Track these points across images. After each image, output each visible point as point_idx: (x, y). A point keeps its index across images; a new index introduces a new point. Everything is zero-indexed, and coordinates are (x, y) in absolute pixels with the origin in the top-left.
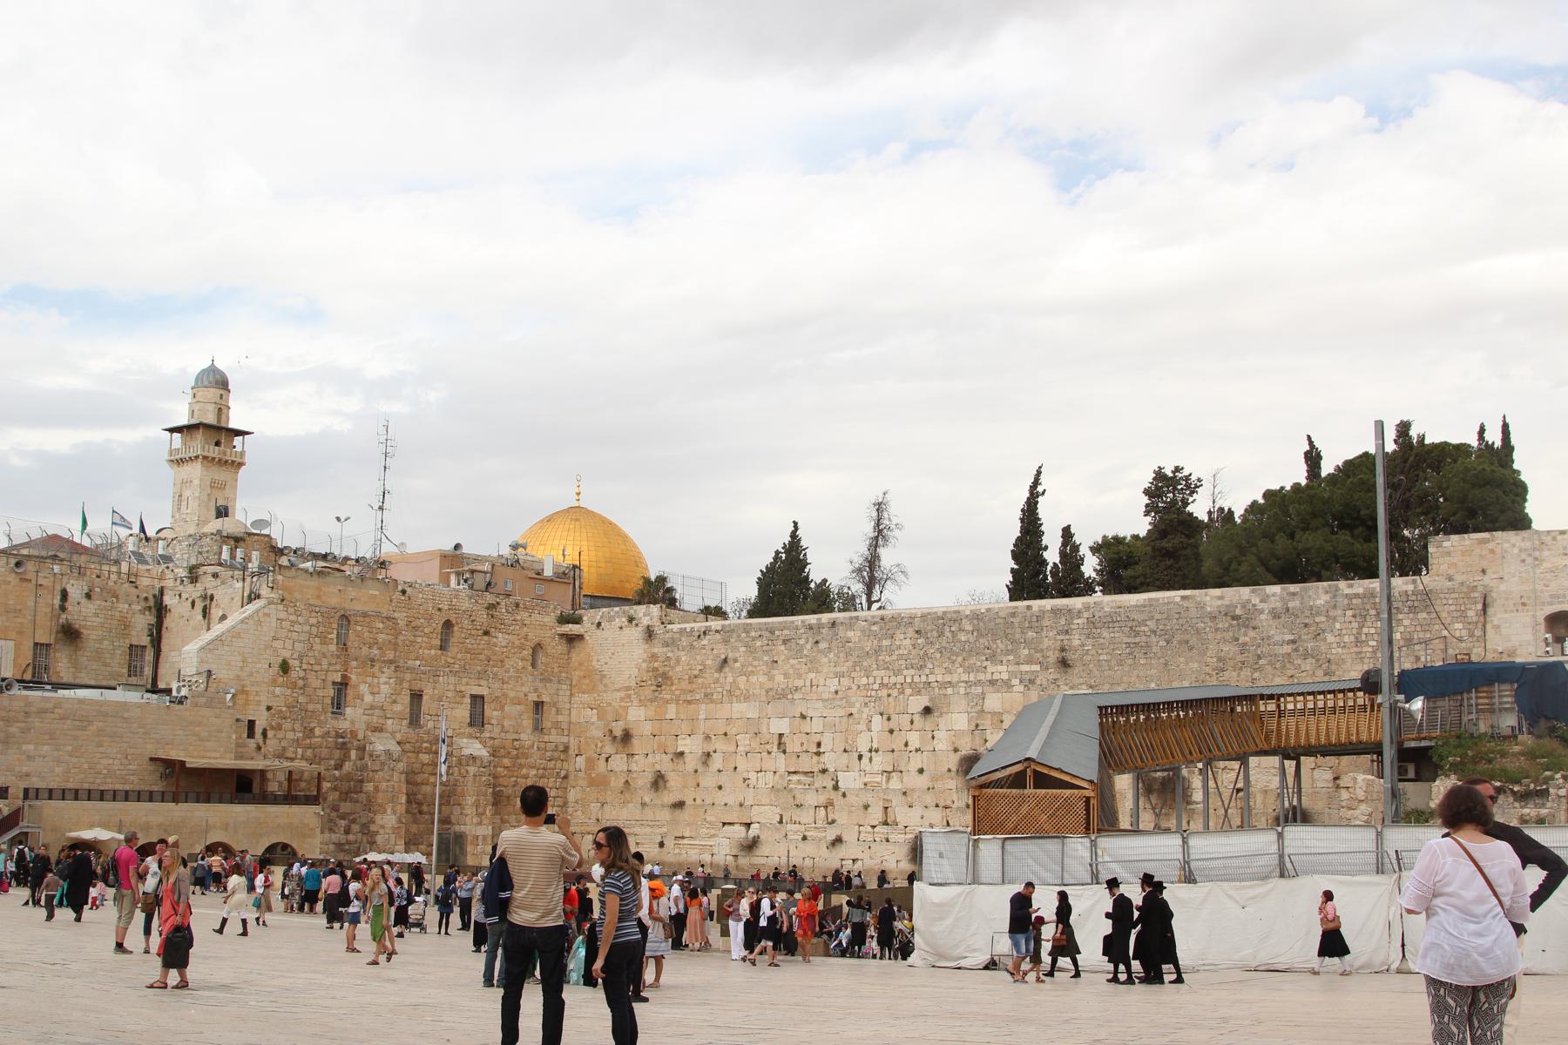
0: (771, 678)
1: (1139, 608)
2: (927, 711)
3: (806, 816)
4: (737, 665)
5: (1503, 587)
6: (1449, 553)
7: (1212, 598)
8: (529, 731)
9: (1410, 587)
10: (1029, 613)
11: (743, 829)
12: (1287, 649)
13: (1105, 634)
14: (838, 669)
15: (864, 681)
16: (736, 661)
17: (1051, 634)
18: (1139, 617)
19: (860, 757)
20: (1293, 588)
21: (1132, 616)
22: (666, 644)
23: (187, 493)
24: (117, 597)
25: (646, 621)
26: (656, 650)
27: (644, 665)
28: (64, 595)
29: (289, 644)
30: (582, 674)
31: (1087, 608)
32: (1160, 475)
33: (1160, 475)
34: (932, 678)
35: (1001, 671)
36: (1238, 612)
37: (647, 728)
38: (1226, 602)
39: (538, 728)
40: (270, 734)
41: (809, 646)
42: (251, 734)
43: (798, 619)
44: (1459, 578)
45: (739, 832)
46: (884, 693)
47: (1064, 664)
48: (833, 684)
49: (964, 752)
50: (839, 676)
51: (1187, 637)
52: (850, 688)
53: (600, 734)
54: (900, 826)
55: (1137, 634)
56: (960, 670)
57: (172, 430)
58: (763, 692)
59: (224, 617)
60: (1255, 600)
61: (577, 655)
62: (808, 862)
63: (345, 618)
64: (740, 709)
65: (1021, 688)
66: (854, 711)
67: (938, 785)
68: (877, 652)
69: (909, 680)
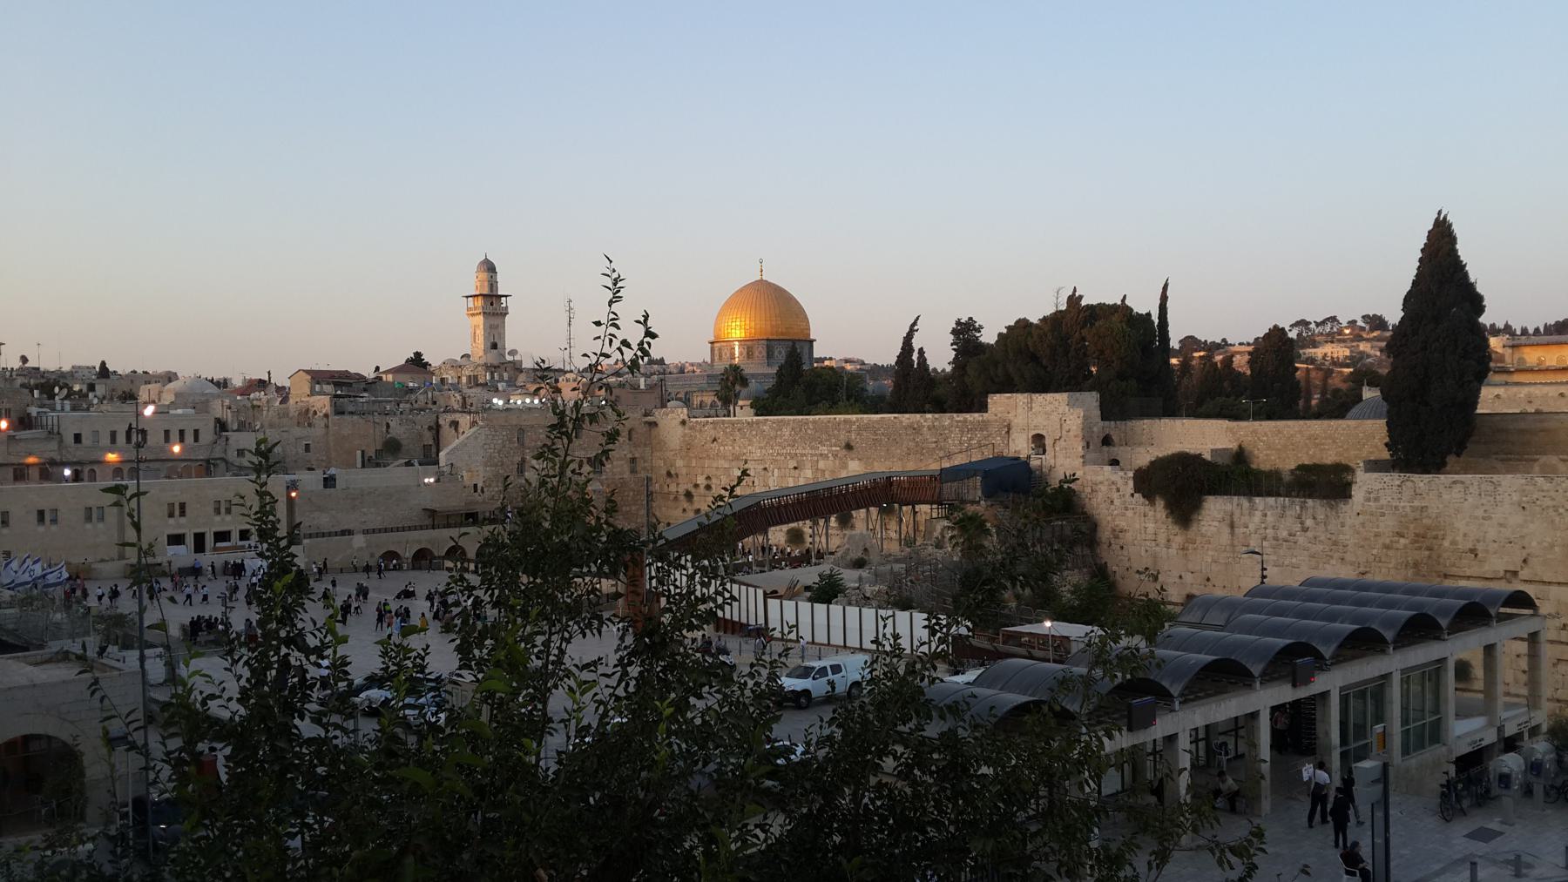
1: (877, 422)
2: (795, 468)
7: (906, 418)
8: (628, 473)
12: (934, 445)
20: (937, 416)
22: (691, 429)
23: (478, 332)
28: (388, 426)
29: (492, 446)
31: (857, 420)
32: (958, 323)
33: (958, 323)
35: (824, 450)
37: (684, 471)
39: (633, 471)
40: (485, 490)
42: (476, 491)
44: (999, 415)
46: (779, 458)
50: (761, 448)
55: (877, 435)
57: (467, 297)
59: (463, 432)
61: (654, 431)
63: (521, 431)
65: (831, 458)
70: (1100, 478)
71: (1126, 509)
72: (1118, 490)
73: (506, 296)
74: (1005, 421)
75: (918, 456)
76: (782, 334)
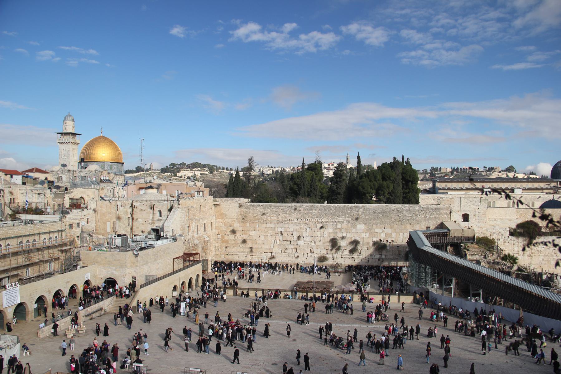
0: (278, 218)
2: (322, 227)
3: (289, 251)
4: (268, 214)
5: (454, 208)
6: (444, 201)
7: (393, 206)
9: (436, 207)
10: (348, 207)
11: (271, 254)
13: (367, 212)
14: (297, 217)
15: (305, 220)
16: (267, 213)
17: (354, 212)
18: (376, 209)
19: (304, 237)
20: (411, 205)
21: (374, 209)
24: (125, 205)
25: (239, 202)
26: (242, 209)
27: (239, 213)
30: (219, 214)
31: (363, 206)
34: (323, 220)
35: (341, 219)
36: (399, 210)
37: (241, 229)
38: (396, 207)
41: (289, 211)
43: (286, 204)
44: (446, 206)
45: (270, 255)
46: (310, 223)
47: (357, 219)
48: (296, 220)
49: (332, 237)
50: (298, 218)
51: (387, 214)
52: (301, 221)
53: (226, 230)
54: (315, 254)
56: (331, 219)
57: (58, 133)
58: (276, 221)
60: (403, 207)
62: (290, 262)
64: (268, 225)
65: (346, 223)
66: (302, 227)
67: (325, 244)
68: (308, 213)
69: (317, 220)
70: (494, 231)
71: (505, 242)
72: (502, 235)
73: (79, 135)
74: (449, 208)
75: (401, 222)
76: (114, 160)
